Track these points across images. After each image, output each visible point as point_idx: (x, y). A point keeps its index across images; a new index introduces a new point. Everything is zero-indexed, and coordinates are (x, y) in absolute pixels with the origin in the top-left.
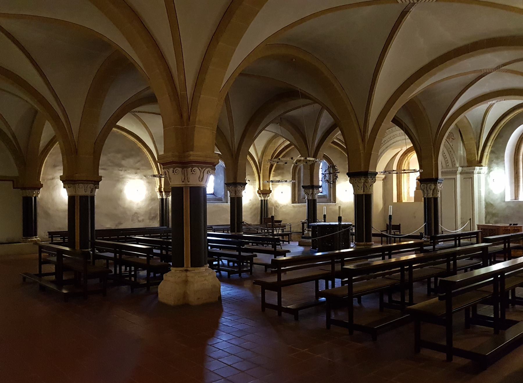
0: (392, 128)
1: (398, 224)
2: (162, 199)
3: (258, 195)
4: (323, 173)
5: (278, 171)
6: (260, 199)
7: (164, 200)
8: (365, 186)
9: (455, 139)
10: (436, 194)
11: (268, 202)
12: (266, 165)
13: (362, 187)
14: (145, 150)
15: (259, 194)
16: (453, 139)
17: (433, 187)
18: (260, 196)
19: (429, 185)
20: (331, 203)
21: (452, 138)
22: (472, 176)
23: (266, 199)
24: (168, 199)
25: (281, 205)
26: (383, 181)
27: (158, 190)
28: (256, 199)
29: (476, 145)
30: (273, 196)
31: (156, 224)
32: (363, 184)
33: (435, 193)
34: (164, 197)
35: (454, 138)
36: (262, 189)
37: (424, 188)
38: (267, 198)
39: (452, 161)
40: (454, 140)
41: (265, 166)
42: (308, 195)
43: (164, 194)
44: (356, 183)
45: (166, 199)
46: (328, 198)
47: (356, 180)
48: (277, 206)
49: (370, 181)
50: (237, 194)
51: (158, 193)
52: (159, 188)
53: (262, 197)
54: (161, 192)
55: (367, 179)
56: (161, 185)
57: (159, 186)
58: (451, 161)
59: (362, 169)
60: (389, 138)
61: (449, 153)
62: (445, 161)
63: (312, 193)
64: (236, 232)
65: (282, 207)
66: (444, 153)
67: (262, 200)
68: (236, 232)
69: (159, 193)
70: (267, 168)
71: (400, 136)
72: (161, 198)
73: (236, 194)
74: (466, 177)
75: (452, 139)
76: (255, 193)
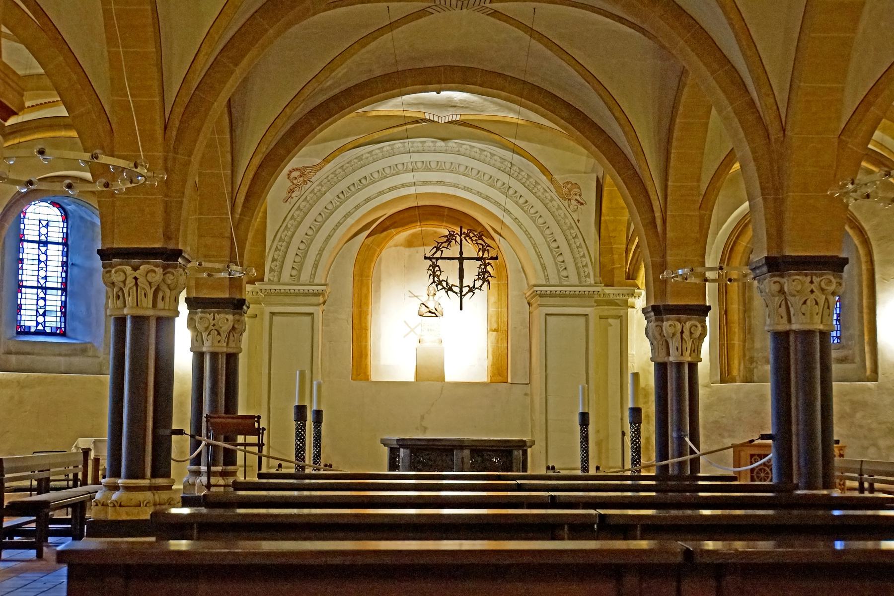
4: (428, 255)
10: (696, 351)
16: (579, 202)
21: (576, 200)
22: (622, 313)
35: (583, 202)
37: (674, 335)
39: (580, 265)
42: (219, 334)
44: (812, 291)
47: (812, 282)
50: (160, 304)
58: (576, 264)
60: (378, 172)
62: (556, 264)
74: (606, 313)
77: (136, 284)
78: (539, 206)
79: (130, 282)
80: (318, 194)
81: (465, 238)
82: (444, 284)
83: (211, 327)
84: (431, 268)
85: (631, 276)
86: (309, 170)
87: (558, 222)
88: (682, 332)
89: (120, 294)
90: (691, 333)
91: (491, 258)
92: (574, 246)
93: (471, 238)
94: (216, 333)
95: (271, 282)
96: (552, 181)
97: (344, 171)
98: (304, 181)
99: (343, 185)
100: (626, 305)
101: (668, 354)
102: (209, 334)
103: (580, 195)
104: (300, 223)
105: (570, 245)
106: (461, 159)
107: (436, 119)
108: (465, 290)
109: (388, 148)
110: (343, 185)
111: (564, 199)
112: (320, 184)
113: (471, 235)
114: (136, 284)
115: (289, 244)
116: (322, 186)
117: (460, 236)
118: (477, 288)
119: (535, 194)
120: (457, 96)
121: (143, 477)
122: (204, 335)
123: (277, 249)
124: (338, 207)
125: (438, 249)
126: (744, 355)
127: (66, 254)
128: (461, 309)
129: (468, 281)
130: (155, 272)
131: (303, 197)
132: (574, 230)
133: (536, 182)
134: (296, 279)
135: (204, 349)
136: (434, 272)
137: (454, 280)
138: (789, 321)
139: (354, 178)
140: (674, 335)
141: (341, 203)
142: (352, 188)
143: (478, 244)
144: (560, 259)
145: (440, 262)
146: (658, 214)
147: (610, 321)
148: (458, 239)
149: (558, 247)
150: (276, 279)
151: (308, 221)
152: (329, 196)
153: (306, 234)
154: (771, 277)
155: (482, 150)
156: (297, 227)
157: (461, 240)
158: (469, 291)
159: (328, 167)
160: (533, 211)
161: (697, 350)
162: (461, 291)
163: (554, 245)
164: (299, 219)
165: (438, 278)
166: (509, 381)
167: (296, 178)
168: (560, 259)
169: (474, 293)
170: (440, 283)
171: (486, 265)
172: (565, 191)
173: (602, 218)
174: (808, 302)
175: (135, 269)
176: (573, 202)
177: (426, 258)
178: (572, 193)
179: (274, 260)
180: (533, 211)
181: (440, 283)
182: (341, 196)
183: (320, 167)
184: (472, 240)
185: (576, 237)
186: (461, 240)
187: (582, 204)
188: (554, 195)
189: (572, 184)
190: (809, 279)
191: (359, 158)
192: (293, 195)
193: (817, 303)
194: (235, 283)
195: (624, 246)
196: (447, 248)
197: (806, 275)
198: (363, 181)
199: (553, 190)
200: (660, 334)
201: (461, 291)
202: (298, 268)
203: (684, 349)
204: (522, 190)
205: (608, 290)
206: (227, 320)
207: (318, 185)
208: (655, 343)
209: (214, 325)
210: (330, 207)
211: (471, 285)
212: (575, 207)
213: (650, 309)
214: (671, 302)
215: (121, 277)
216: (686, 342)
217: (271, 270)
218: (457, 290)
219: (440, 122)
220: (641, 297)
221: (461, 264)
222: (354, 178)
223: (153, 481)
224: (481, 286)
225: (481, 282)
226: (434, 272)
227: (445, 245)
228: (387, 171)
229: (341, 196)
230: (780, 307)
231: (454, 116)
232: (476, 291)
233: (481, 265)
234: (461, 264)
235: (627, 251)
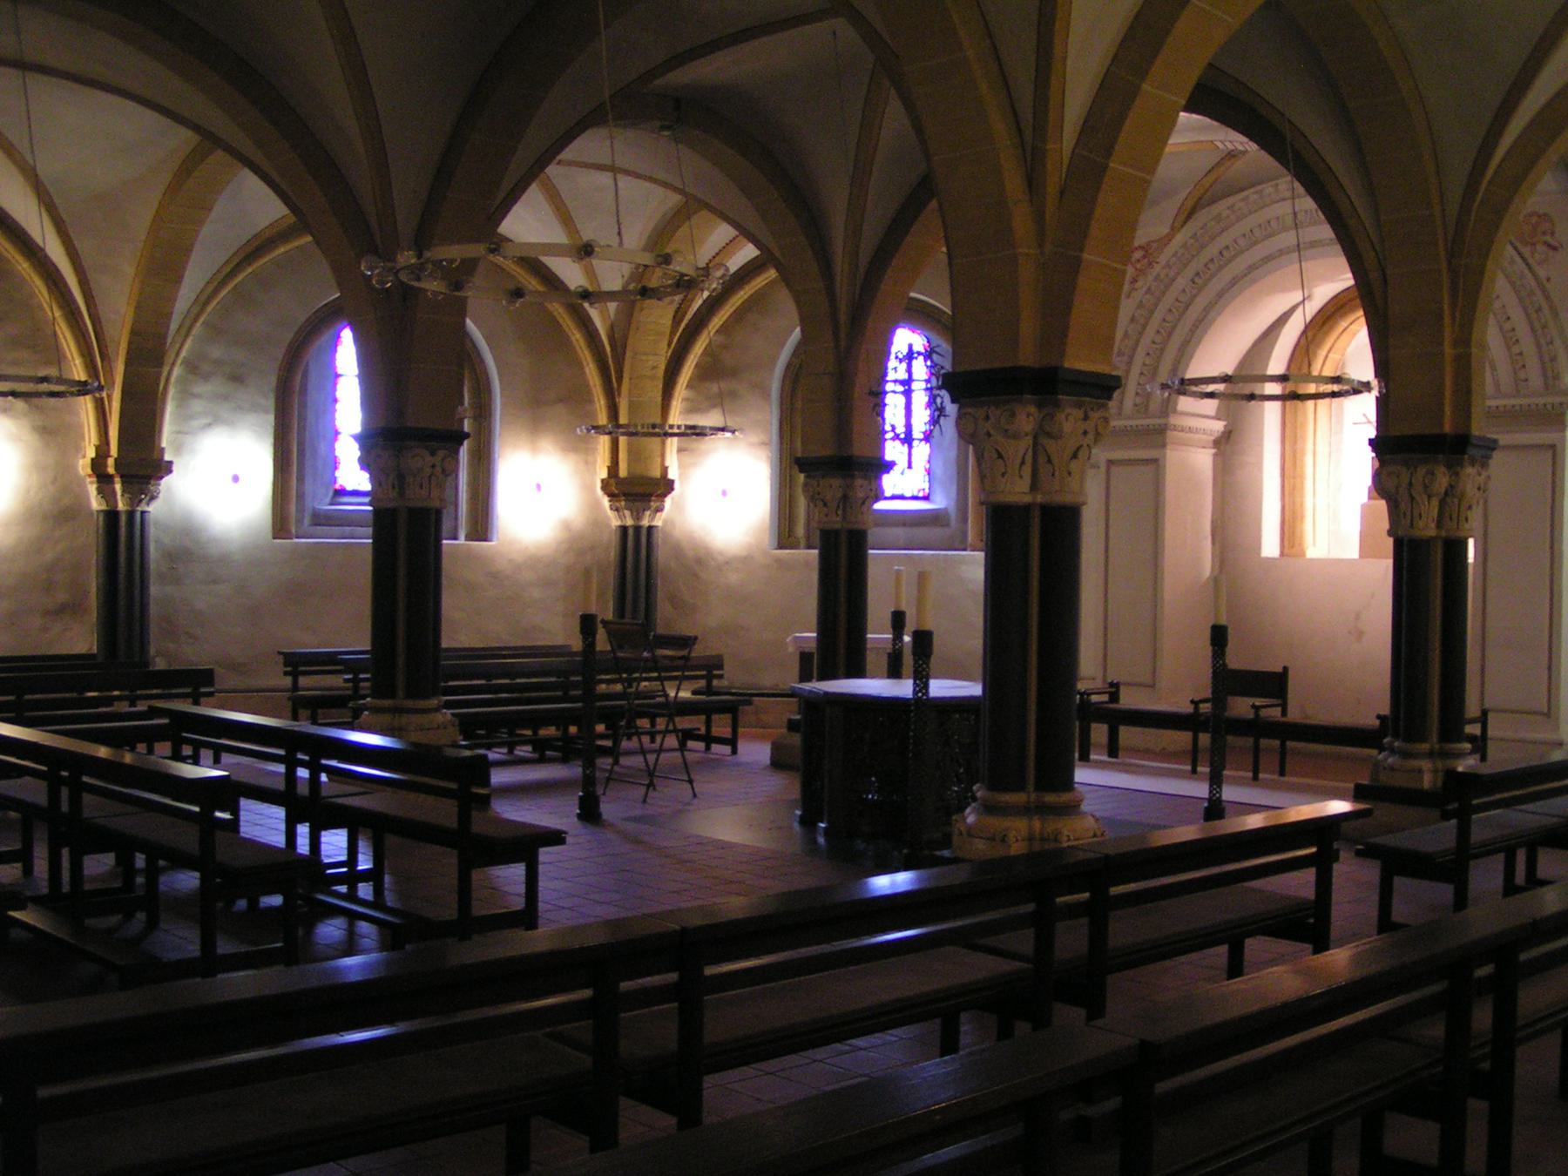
0: (1259, 187)
1: (1279, 669)
2: (111, 516)
3: (606, 501)
5: (708, 384)
6: (615, 522)
7: (123, 519)
8: (1042, 459)
9: (1562, 246)
11: (659, 539)
12: (645, 354)
13: (1023, 463)
14: (23, 266)
15: (611, 495)
17: (1442, 480)
18: (617, 510)
19: (1421, 471)
20: (965, 550)
21: (1545, 243)
23: (645, 522)
24: (143, 513)
25: (721, 553)
26: (1213, 451)
27: (89, 471)
28: (596, 523)
30: (679, 506)
31: (81, 639)
32: (1029, 441)
33: (1451, 519)
34: (121, 506)
35: (1556, 244)
36: (623, 472)
38: (653, 519)
41: (644, 358)
42: (825, 505)
43: (118, 487)
44: (989, 435)
45: (131, 514)
46: (953, 522)
47: (987, 418)
48: (699, 561)
49: (1067, 427)
51: (91, 483)
52: (92, 460)
53: (627, 513)
54: (103, 479)
55: (1052, 416)
56: (108, 443)
57: (98, 448)
59: (1027, 356)
63: (845, 497)
64: (400, 693)
65: (727, 563)
67: (624, 529)
68: (400, 693)
69: (95, 486)
70: (654, 368)
72: (104, 507)
73: (402, 494)
75: (1545, 248)
76: (588, 488)
86: (1154, 245)
88: (1410, 484)
92: (1537, 325)
94: (821, 503)
97: (1197, 240)
98: (1150, 264)
103: (1553, 234)
109: (1255, 196)
115: (1131, 357)
121: (393, 695)
124: (1195, 296)
139: (1212, 250)
141: (1200, 290)
152: (1181, 282)
153: (1154, 342)
156: (1141, 334)
159: (1180, 238)
164: (1142, 321)
167: (1139, 261)
176: (1540, 247)
183: (1169, 238)
187: (1555, 249)
191: (1218, 218)
203: (1416, 513)
207: (1164, 268)
210: (1183, 298)
216: (1418, 504)
228: (1257, 232)
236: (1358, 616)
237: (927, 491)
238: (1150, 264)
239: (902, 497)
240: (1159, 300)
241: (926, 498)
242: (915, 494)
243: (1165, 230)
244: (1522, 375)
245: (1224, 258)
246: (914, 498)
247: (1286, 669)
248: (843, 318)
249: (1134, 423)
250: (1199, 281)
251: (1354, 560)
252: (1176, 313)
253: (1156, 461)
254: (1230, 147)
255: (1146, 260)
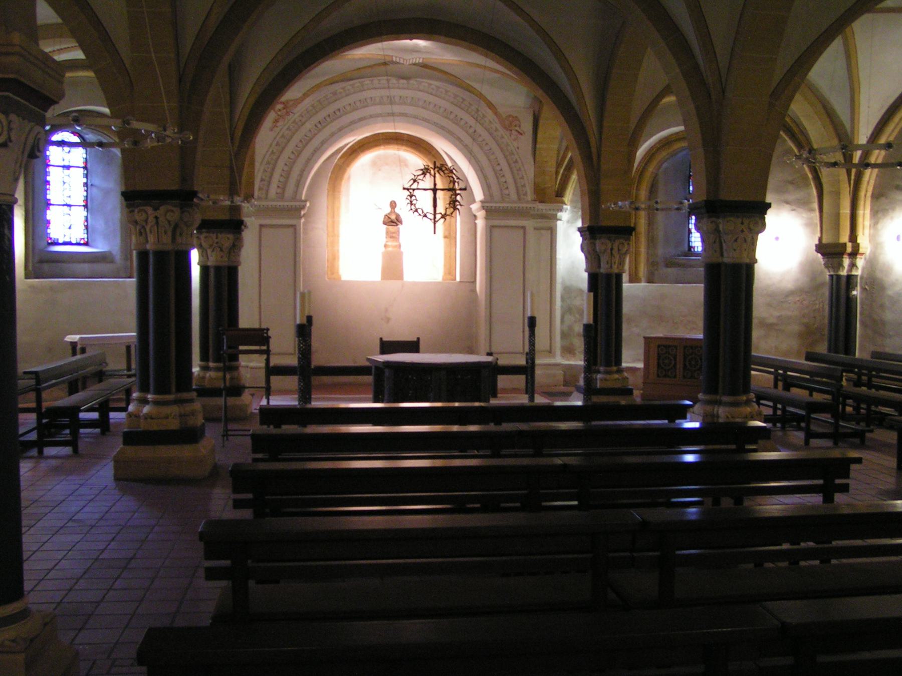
0: (363, 80)
1: (415, 339)
4: (407, 186)
9: (524, 134)
16: (519, 132)
21: (517, 131)
29: (558, 156)
35: (522, 132)
40: (522, 137)
42: (221, 250)
61: (509, 165)
62: (499, 184)
63: (234, 246)
66: (499, 164)
71: (381, 103)
74: (539, 225)
75: (517, 133)
77: (157, 223)
78: (485, 135)
79: (151, 219)
80: (299, 123)
81: (438, 171)
82: (420, 211)
83: (215, 245)
84: (409, 197)
85: (560, 193)
86: (291, 103)
87: (501, 149)
88: (612, 249)
89: (142, 231)
90: (619, 250)
91: (461, 189)
93: (443, 171)
94: (219, 249)
95: (259, 198)
96: (496, 113)
98: (287, 112)
99: (320, 116)
100: (555, 218)
101: (599, 267)
102: (213, 251)
103: (520, 126)
104: (283, 149)
105: (511, 169)
106: (420, 94)
107: (402, 61)
108: (438, 216)
110: (320, 116)
111: (507, 130)
112: (301, 116)
113: (444, 169)
114: (157, 223)
116: (302, 117)
117: (434, 169)
118: (448, 215)
119: (482, 125)
120: (421, 43)
121: (168, 392)
122: (209, 252)
123: (265, 171)
124: (315, 135)
125: (415, 181)
126: (648, 260)
127: (86, 176)
128: (435, 233)
129: (441, 209)
130: (172, 211)
131: (286, 127)
132: (514, 155)
133: (483, 114)
134: (281, 196)
135: (209, 264)
136: (411, 202)
137: (429, 209)
138: (722, 255)
139: (330, 109)
140: (605, 251)
142: (328, 119)
143: (449, 177)
144: (503, 180)
145: (416, 193)
146: (594, 150)
147: (543, 232)
148: (432, 172)
149: (501, 170)
150: (263, 196)
151: (291, 146)
152: (308, 126)
154: (710, 217)
155: (438, 87)
156: (281, 152)
157: (435, 174)
158: (442, 218)
160: (480, 139)
161: (622, 263)
162: (435, 218)
163: (498, 168)
165: (415, 206)
166: (458, 279)
167: (280, 110)
168: (503, 180)
169: (445, 219)
170: (416, 210)
171: (456, 195)
172: (507, 123)
173: (538, 146)
174: (739, 240)
175: (156, 209)
176: (514, 132)
177: (404, 189)
178: (514, 124)
179: (262, 180)
180: (480, 139)
181: (416, 210)
182: (319, 126)
184: (444, 173)
185: (516, 162)
186: (435, 174)
187: (521, 134)
188: (499, 126)
189: (513, 117)
190: (740, 220)
192: (278, 124)
193: (745, 241)
194: (236, 209)
195: (554, 170)
196: (422, 180)
197: (738, 217)
198: (338, 113)
199: (497, 121)
200: (594, 250)
201: (435, 218)
202: (283, 187)
204: (472, 122)
205: (541, 207)
206: (228, 239)
208: (589, 257)
209: (217, 243)
210: (309, 135)
211: (443, 213)
212: (515, 137)
213: (586, 229)
214: (606, 223)
215: (144, 216)
216: (614, 257)
217: (260, 189)
218: (432, 217)
219: (405, 63)
220: (567, 212)
221: (435, 194)
222: (330, 109)
223: (179, 395)
224: (452, 213)
225: (452, 210)
226: (411, 202)
227: (421, 177)
228: (358, 104)
229: (319, 126)
230: (715, 242)
231: (418, 59)
232: (448, 218)
233: (452, 195)
234: (435, 194)
235: (557, 173)
236: (386, 310)
237: (86, 240)
238: (288, 113)
239: (70, 244)
240: (294, 134)
241: (86, 244)
242: (78, 241)
243: (299, 95)
244: (506, 192)
245: (336, 115)
246: (78, 244)
247: (418, 339)
248: (238, 133)
249: (274, 203)
250: (320, 126)
251: (377, 282)
252: (304, 142)
253: (295, 225)
254: (398, 61)
255: (285, 110)
